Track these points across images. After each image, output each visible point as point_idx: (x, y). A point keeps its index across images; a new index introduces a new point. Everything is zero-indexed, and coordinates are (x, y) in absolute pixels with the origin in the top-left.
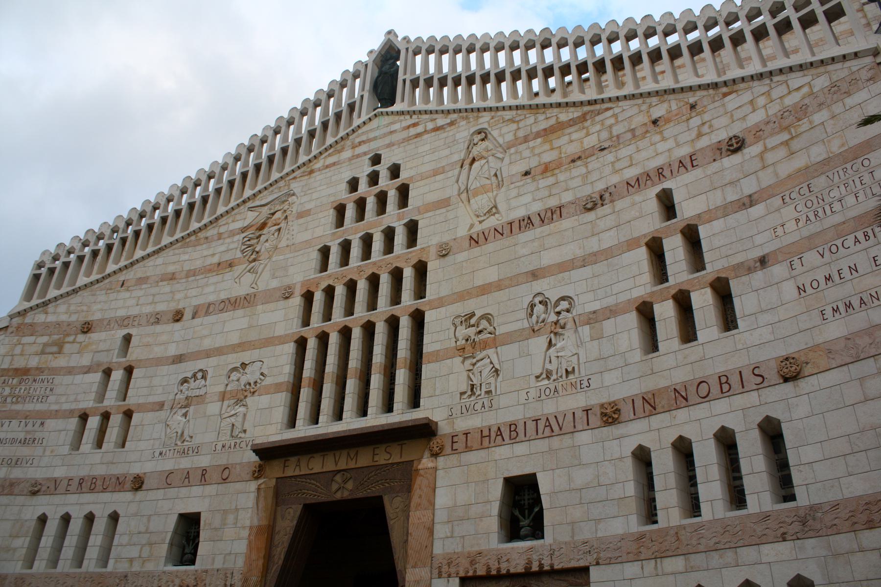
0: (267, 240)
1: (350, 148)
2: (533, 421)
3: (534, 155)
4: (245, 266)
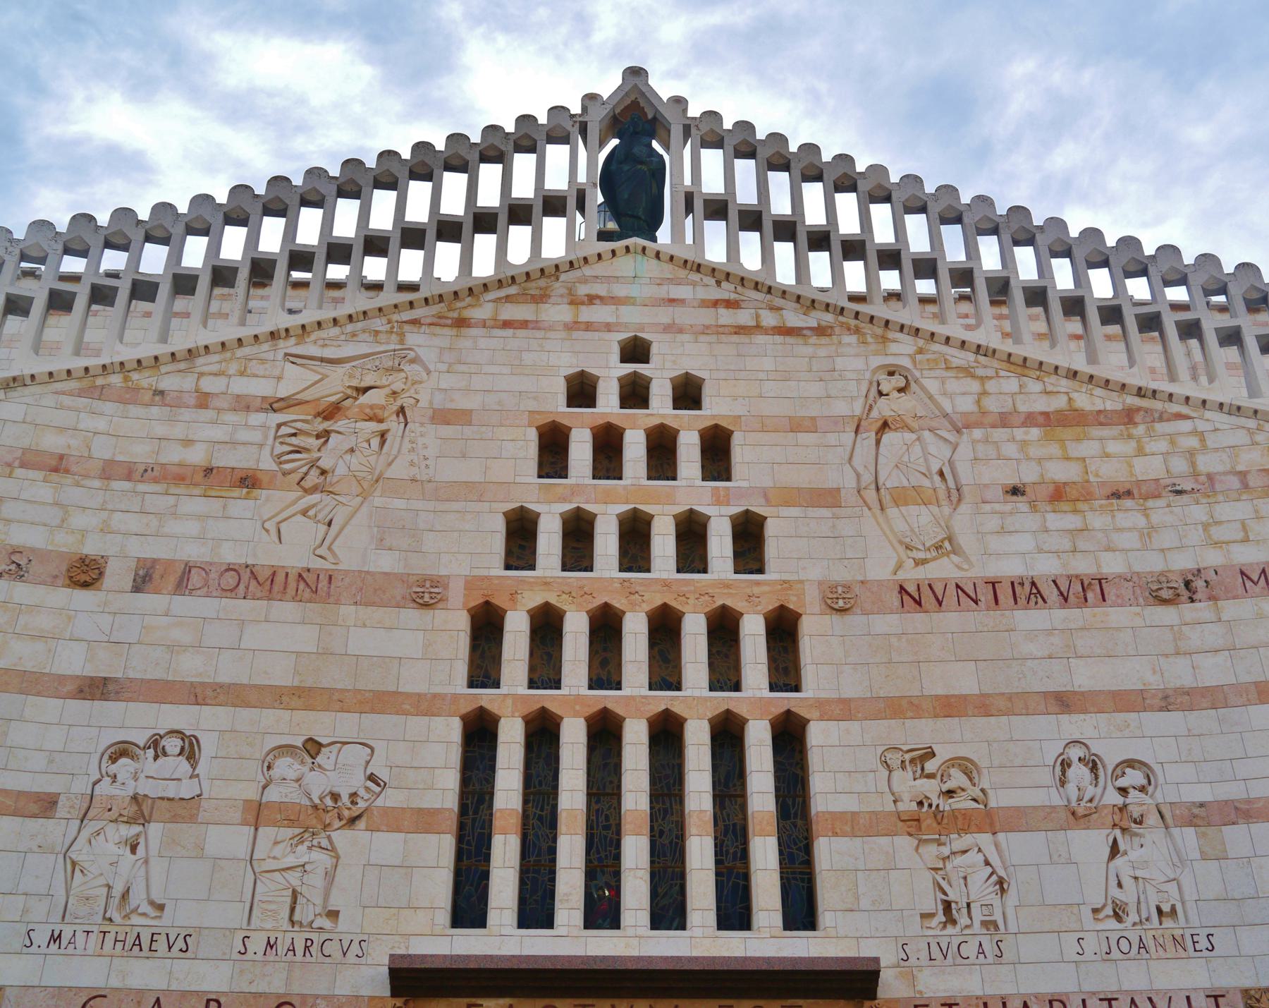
0: (352, 450)
1: (565, 300)
2: (1101, 1000)
3: (1029, 459)
4: (293, 495)
